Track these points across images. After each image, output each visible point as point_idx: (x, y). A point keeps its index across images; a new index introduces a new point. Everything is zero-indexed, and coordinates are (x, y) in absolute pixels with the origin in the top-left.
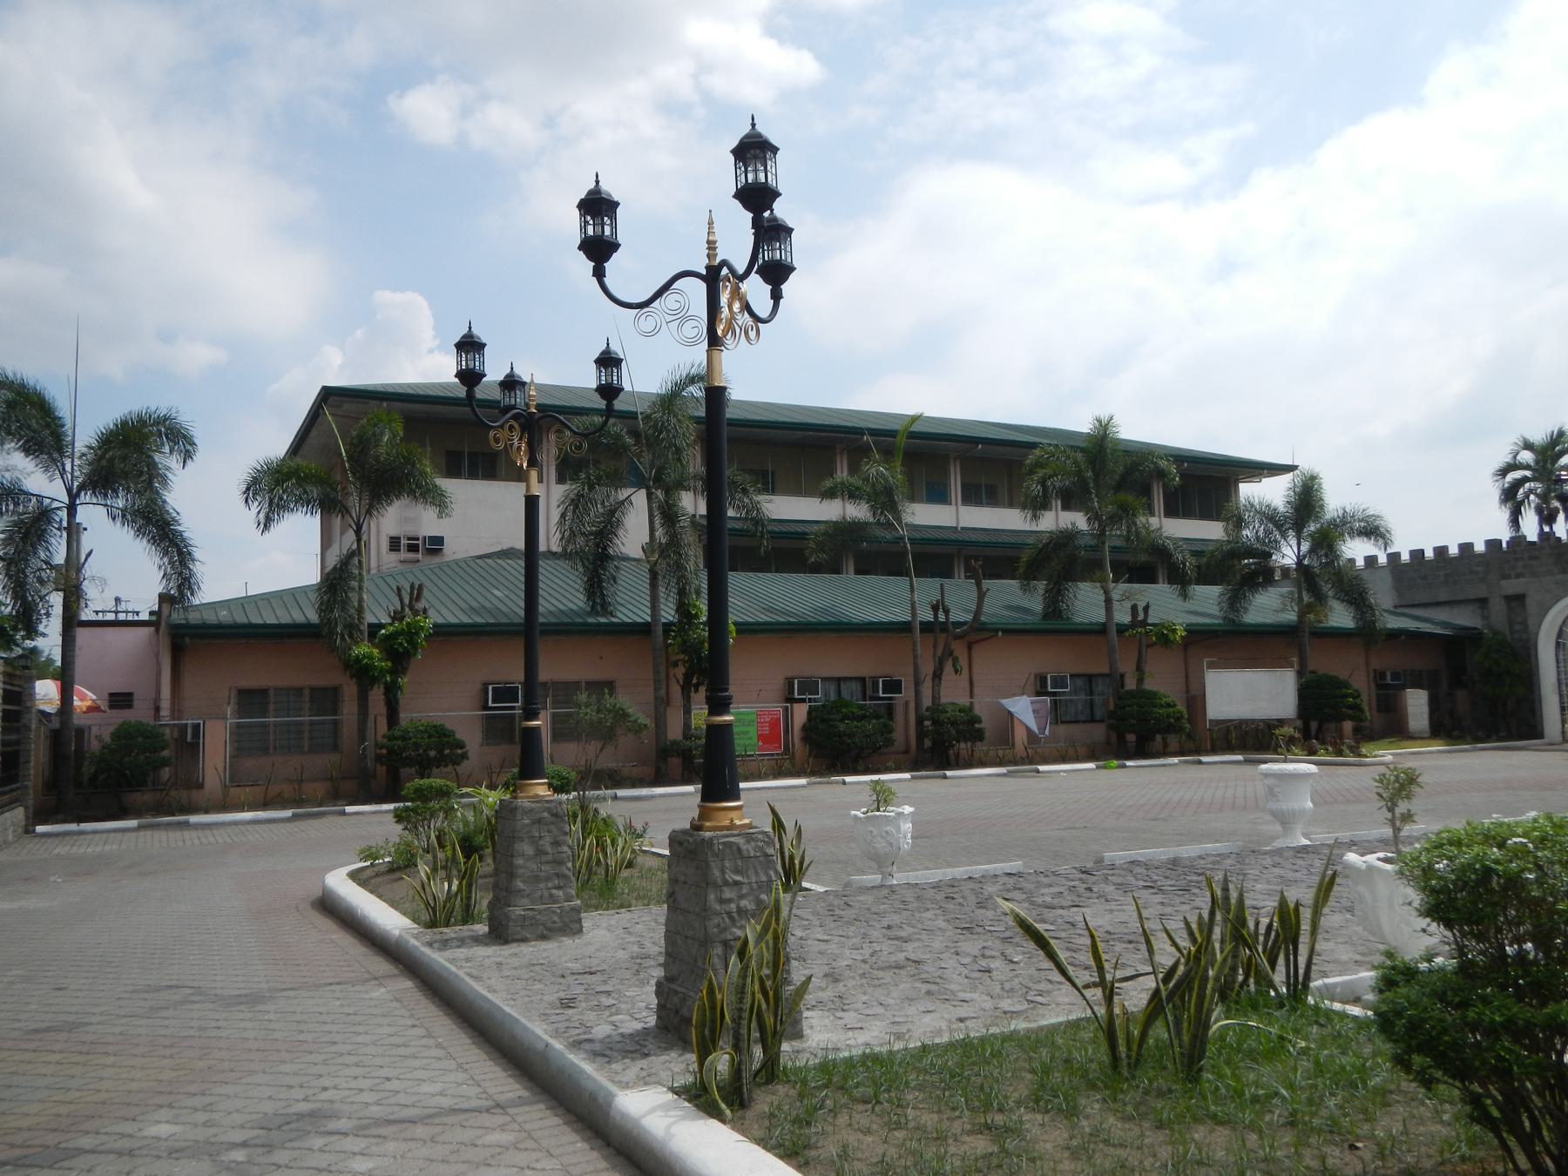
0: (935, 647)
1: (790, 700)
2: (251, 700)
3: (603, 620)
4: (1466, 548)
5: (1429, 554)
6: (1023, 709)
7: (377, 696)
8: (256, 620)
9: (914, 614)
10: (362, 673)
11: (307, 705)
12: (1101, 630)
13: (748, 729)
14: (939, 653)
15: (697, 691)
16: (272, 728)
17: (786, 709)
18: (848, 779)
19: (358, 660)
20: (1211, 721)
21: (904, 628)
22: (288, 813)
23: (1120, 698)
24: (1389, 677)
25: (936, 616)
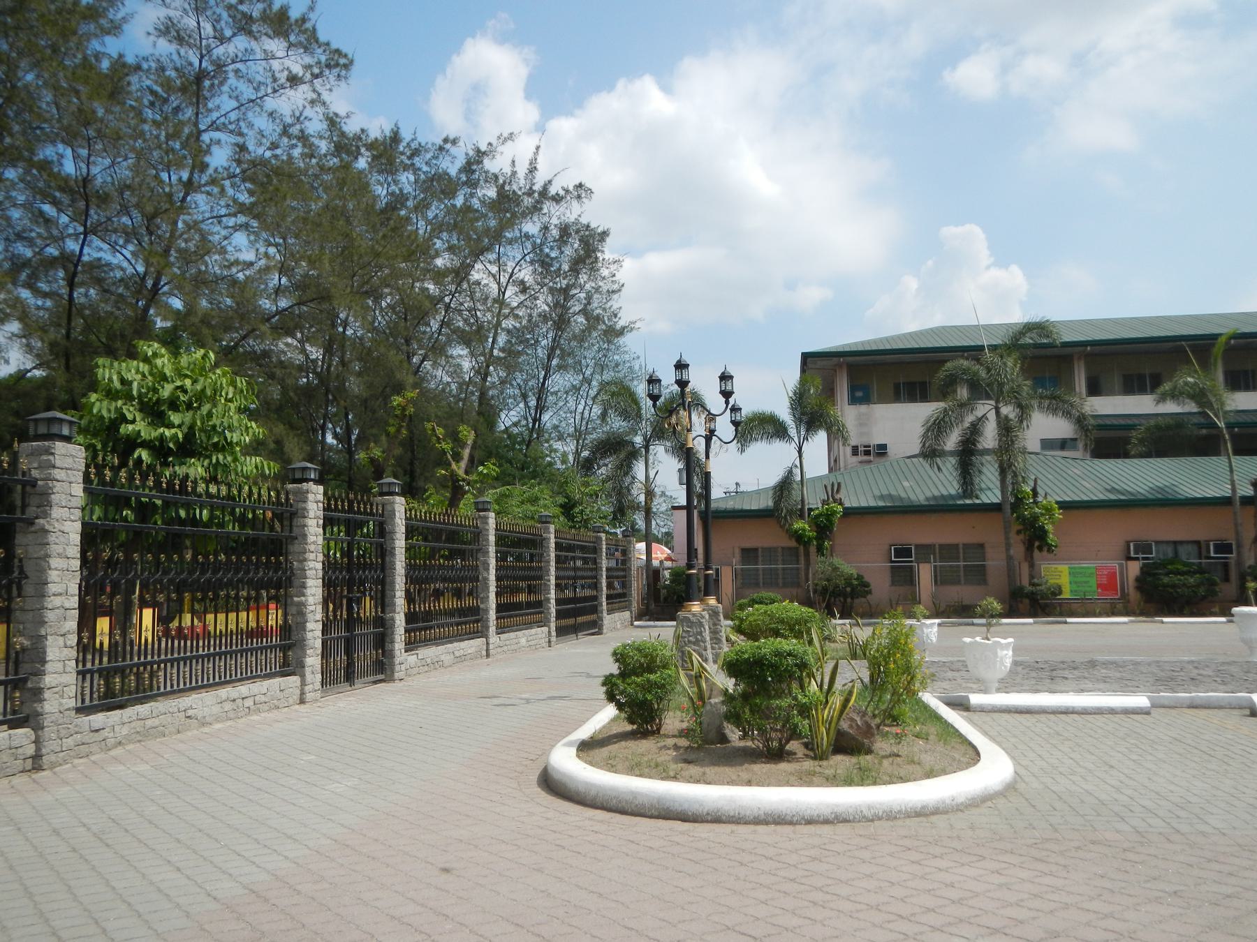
1: (1129, 558)
2: (749, 554)
3: (968, 502)
8: (747, 507)
9: (1234, 490)
10: (798, 537)
11: (780, 558)
13: (1088, 579)
16: (761, 572)
17: (1121, 566)
18: (1166, 620)
19: (796, 532)
21: (1226, 502)
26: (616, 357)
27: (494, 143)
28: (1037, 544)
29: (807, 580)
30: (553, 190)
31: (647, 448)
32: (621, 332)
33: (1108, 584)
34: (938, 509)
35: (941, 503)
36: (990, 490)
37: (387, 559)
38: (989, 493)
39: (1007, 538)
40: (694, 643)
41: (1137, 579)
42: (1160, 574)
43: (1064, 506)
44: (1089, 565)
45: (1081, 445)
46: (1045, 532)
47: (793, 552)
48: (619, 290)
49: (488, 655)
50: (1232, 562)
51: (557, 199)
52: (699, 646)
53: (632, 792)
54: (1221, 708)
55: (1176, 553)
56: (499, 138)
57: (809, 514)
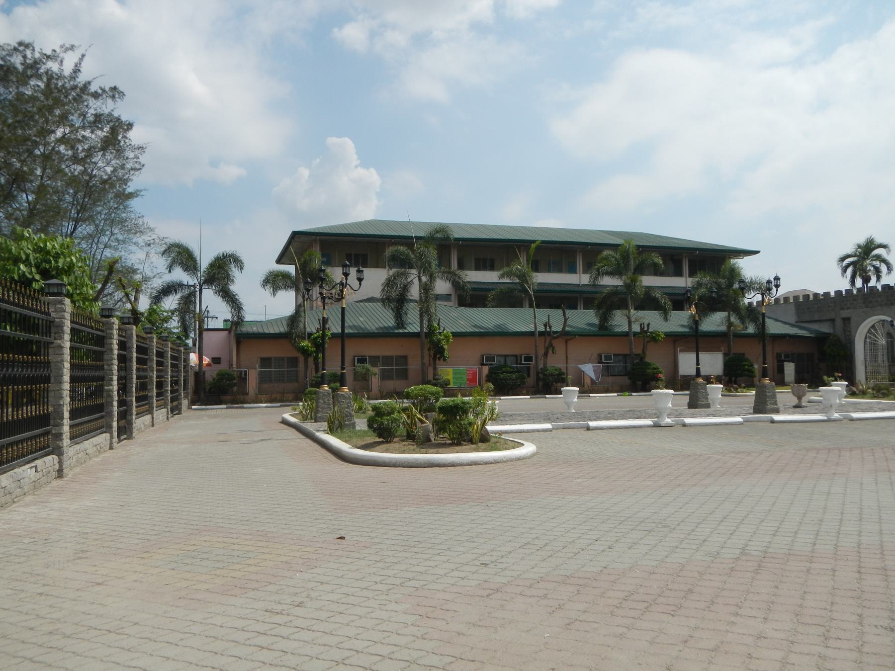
0: (545, 342)
1: (483, 364)
2: (265, 362)
3: (401, 331)
4: (827, 294)
5: (833, 294)
6: (589, 370)
7: (311, 360)
8: (267, 331)
10: (305, 352)
11: (286, 364)
12: (626, 334)
14: (547, 344)
15: (439, 360)
17: (479, 368)
19: (303, 347)
20: (681, 376)
21: (531, 334)
22: (279, 404)
23: (634, 365)
24: (783, 357)
25: (546, 329)
26: (124, 215)
27: (58, 50)
28: (438, 356)
29: (306, 377)
30: (93, 88)
31: (201, 291)
32: (131, 196)
34: (383, 335)
35: (386, 331)
36: (413, 324)
37: (128, 364)
38: (411, 326)
39: (422, 353)
40: (347, 408)
41: (487, 376)
42: (498, 373)
43: (455, 335)
45: (453, 297)
46: (444, 349)
47: (293, 362)
48: (140, 169)
49: (153, 425)
50: (532, 367)
51: (96, 95)
52: (349, 409)
53: (415, 459)
54: (574, 428)
55: (505, 361)
56: (62, 47)
57: (309, 337)
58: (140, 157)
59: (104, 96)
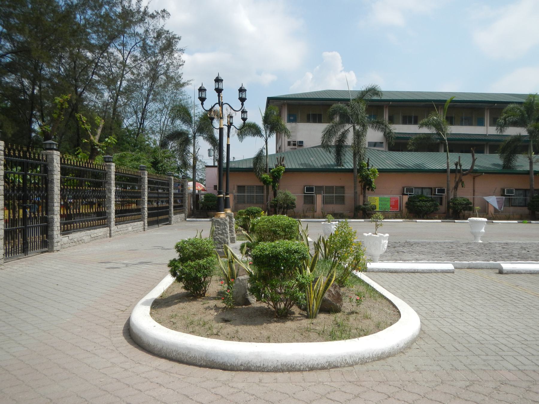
0: (456, 178)
1: (403, 194)
2: (241, 188)
3: (339, 168)
6: (493, 201)
7: (270, 187)
9: (448, 166)
10: (265, 181)
11: (255, 191)
12: (528, 173)
13: (387, 203)
14: (457, 180)
15: (368, 190)
16: (246, 197)
17: (400, 197)
18: (417, 221)
19: (263, 178)
21: (444, 171)
23: (533, 198)
25: (456, 167)
26: (180, 97)
28: (367, 187)
29: (267, 201)
30: (150, 11)
31: (194, 137)
32: (183, 85)
33: (395, 204)
34: (326, 170)
35: (328, 167)
36: (349, 163)
37: (49, 185)
38: (347, 164)
39: (355, 184)
40: (221, 234)
41: (407, 203)
42: (416, 201)
43: (381, 171)
44: (387, 197)
45: (384, 144)
46: (371, 182)
47: (261, 188)
48: (183, 65)
49: (110, 236)
50: (444, 197)
51: (153, 16)
52: (224, 236)
53: (187, 348)
54: (482, 268)
55: (422, 192)
57: (269, 171)
58: (182, 56)
59: (158, 17)
